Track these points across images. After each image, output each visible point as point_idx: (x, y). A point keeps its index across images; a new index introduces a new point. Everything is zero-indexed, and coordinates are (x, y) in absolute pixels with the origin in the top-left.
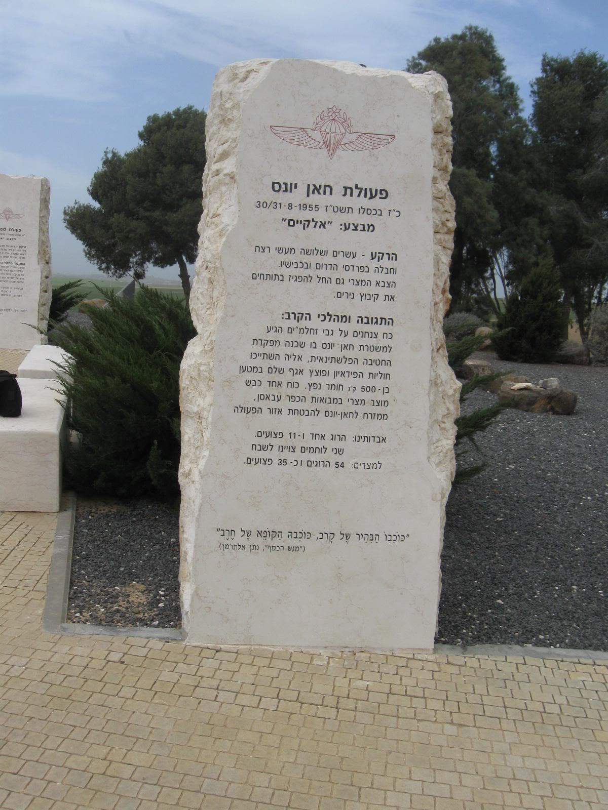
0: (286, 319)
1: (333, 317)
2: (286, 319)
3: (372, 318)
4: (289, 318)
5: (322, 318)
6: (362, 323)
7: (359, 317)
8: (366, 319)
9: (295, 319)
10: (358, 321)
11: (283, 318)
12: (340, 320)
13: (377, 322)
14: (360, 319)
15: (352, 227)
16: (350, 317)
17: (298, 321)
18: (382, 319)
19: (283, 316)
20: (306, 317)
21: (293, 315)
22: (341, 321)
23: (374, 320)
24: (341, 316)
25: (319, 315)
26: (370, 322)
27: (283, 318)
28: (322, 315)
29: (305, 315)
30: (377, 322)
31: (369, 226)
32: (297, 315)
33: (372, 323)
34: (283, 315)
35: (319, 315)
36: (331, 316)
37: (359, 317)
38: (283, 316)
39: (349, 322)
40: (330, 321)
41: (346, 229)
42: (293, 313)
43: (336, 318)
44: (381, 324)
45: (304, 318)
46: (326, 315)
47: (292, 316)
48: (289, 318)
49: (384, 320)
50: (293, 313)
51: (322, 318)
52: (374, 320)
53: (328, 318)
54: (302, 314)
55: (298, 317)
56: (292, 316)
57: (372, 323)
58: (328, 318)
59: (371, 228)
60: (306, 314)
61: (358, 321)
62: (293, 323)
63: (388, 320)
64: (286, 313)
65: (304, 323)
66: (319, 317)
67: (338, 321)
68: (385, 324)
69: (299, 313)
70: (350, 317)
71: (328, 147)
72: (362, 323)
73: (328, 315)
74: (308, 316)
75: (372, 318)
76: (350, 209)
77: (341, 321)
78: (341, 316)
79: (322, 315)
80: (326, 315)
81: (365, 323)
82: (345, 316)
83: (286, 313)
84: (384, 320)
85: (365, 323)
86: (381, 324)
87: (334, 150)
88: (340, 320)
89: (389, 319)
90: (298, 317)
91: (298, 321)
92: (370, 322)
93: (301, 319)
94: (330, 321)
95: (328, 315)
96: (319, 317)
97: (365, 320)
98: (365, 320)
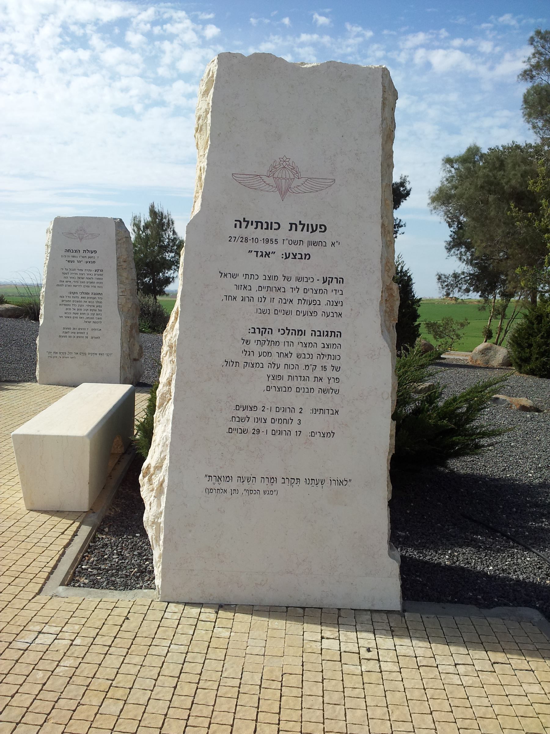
0: (252, 333)
1: (291, 331)
2: (252, 333)
3: (324, 331)
4: (255, 332)
5: (282, 332)
6: (315, 336)
7: (312, 331)
9: (259, 333)
10: (312, 334)
11: (249, 332)
12: (297, 334)
13: (327, 335)
14: (313, 332)
16: (305, 331)
17: (262, 335)
19: (250, 331)
22: (298, 335)
23: (326, 333)
25: (279, 329)
26: (322, 334)
27: (249, 332)
28: (282, 329)
29: (267, 330)
30: (327, 335)
32: (261, 330)
33: (323, 336)
34: (249, 329)
35: (279, 329)
36: (289, 330)
37: (312, 331)
38: (250, 331)
39: (305, 335)
42: (257, 328)
43: (294, 332)
45: (267, 332)
47: (257, 331)
48: (255, 332)
49: (333, 333)
50: (257, 328)
51: (282, 332)
52: (326, 333)
54: (266, 329)
55: (262, 331)
56: (257, 331)
57: (323, 336)
61: (312, 334)
62: (258, 336)
63: (336, 333)
64: (252, 328)
65: (266, 336)
66: (279, 331)
67: (295, 335)
68: (335, 336)
70: (305, 331)
71: (281, 193)
72: (315, 336)
73: (287, 329)
74: (270, 330)
75: (324, 331)
76: (301, 242)
77: (298, 335)
79: (282, 329)
80: (285, 330)
81: (318, 336)
82: (301, 330)
83: (252, 328)
84: (333, 333)
85: (318, 336)
87: (285, 193)
88: (297, 334)
89: (337, 332)
90: (262, 331)
91: (262, 335)
92: (322, 334)
93: (265, 333)
94: (288, 335)
95: (287, 329)
96: (279, 331)
97: (318, 333)
98: (318, 333)
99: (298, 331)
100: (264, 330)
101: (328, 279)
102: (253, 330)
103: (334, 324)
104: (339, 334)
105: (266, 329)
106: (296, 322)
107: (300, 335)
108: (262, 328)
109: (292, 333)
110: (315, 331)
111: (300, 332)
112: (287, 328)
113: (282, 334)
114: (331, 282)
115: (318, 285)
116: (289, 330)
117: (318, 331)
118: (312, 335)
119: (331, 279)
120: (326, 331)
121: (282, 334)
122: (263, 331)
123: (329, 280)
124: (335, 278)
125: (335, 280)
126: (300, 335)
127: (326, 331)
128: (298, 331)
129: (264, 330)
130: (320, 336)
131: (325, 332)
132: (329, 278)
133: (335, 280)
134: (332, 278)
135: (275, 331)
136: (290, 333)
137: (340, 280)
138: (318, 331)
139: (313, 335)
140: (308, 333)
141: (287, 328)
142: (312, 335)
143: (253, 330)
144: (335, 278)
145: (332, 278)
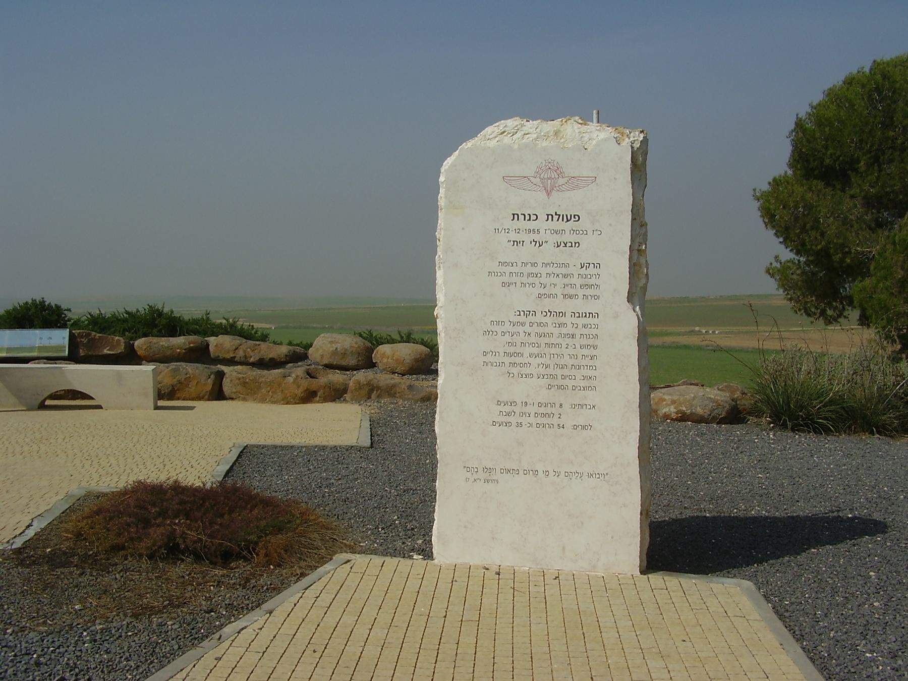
1: (553, 313)
14: (573, 314)
15: (563, 244)
18: (589, 313)
20: (532, 314)
23: (584, 315)
29: (531, 312)
30: (586, 316)
31: (575, 243)
32: (526, 312)
36: (551, 312)
41: (558, 246)
43: (555, 314)
45: (531, 314)
47: (522, 313)
48: (520, 315)
49: (591, 315)
52: (584, 315)
53: (549, 314)
54: (530, 312)
56: (522, 313)
58: (549, 314)
59: (577, 245)
62: (522, 318)
82: (562, 312)
84: (591, 315)
95: (549, 311)
97: (577, 315)
100: (528, 313)
101: (585, 265)
103: (592, 307)
104: (596, 315)
105: (530, 312)
106: (558, 305)
116: (551, 312)
119: (588, 265)
122: (527, 313)
130: (579, 317)
134: (589, 264)
136: (552, 315)
137: (597, 266)
140: (568, 315)
145: (589, 264)
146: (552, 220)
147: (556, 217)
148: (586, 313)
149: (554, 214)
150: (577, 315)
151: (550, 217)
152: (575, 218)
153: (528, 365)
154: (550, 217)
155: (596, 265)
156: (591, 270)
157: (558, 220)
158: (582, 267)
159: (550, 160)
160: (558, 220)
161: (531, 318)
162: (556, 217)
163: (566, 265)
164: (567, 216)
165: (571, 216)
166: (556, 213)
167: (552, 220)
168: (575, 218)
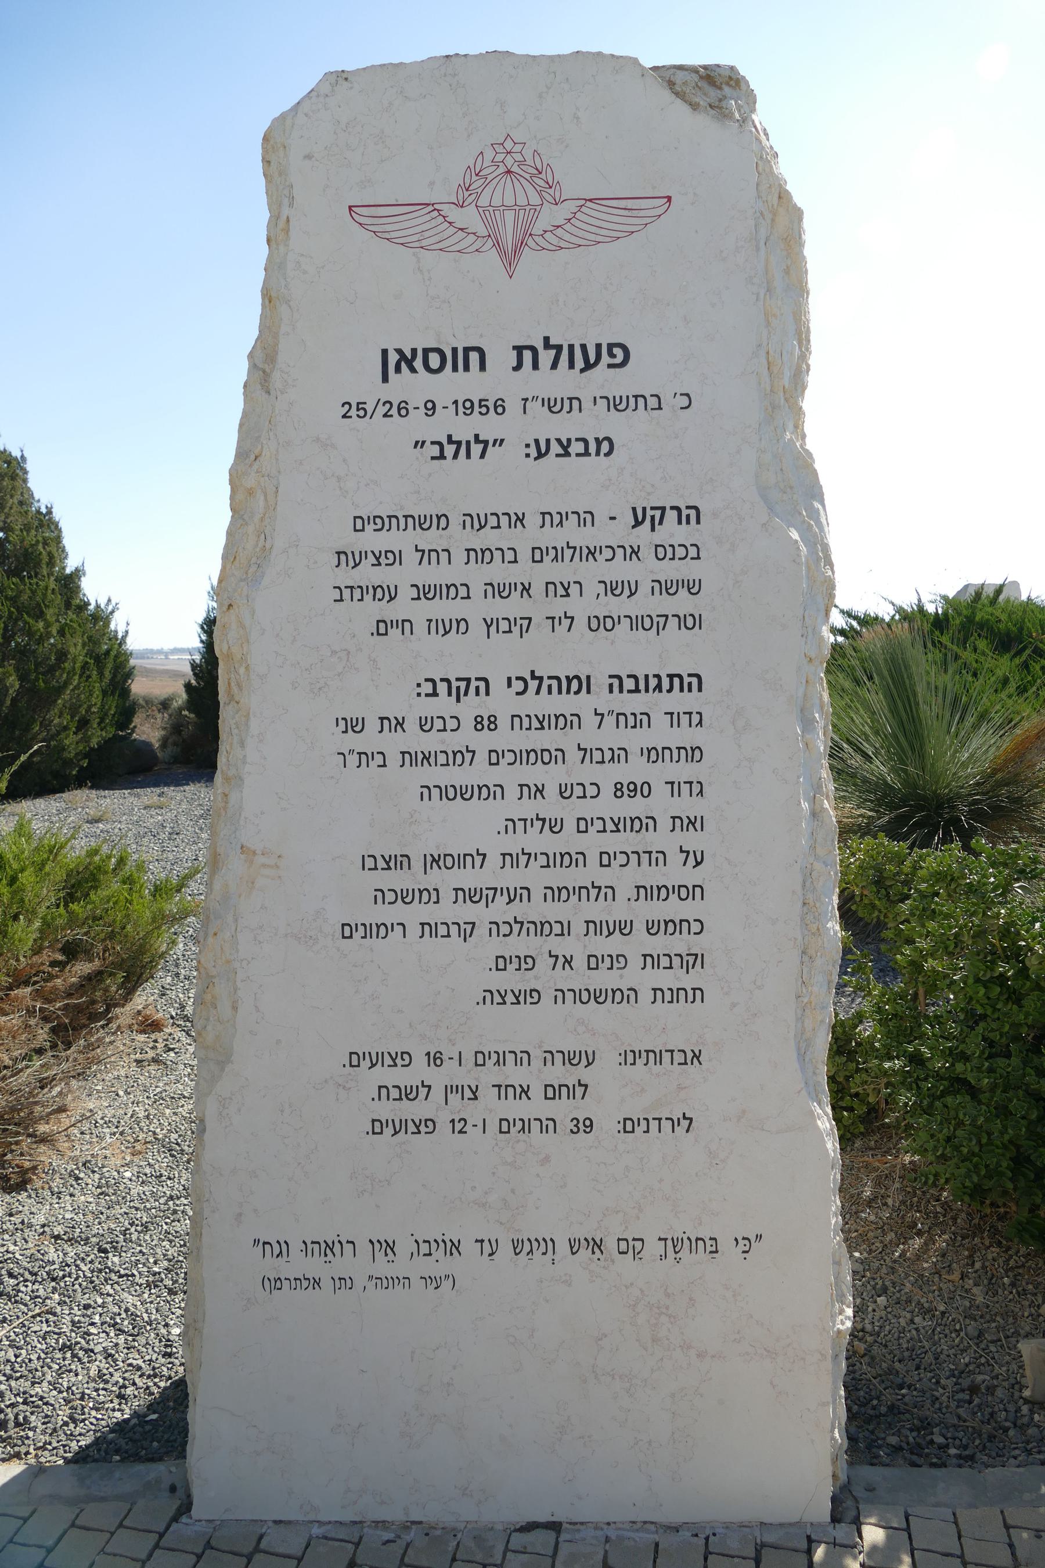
0: (427, 695)
1: (546, 682)
2: (427, 695)
3: (647, 676)
4: (435, 694)
5: (519, 686)
7: (610, 677)
8: (632, 680)
9: (450, 694)
10: (611, 686)
11: (419, 695)
13: (659, 687)
14: (616, 682)
17: (458, 700)
18: (671, 677)
19: (419, 690)
21: (445, 684)
22: (568, 692)
23: (653, 683)
24: (567, 677)
26: (642, 686)
27: (419, 695)
28: (518, 678)
29: (474, 684)
30: (659, 687)
32: (455, 684)
33: (647, 690)
34: (419, 685)
35: (509, 679)
36: (541, 679)
38: (419, 690)
39: (589, 692)
40: (538, 692)
42: (442, 680)
43: (554, 683)
44: (670, 691)
45: (472, 690)
46: (528, 677)
47: (442, 687)
48: (435, 694)
49: (676, 681)
50: (442, 680)
51: (519, 686)
52: (653, 683)
53: (533, 685)
55: (458, 688)
56: (442, 687)
57: (647, 690)
58: (533, 685)
60: (477, 679)
61: (611, 686)
62: (444, 704)
63: (686, 680)
64: (427, 680)
66: (509, 685)
67: (560, 692)
68: (682, 690)
69: (458, 679)
70: (588, 678)
72: (621, 691)
74: (482, 685)
75: (647, 676)
77: (568, 692)
78: (567, 677)
79: (518, 678)
80: (528, 677)
81: (629, 691)
83: (427, 680)
84: (676, 681)
85: (629, 691)
86: (670, 691)
89: (690, 675)
90: (458, 688)
91: (458, 700)
92: (642, 686)
93: (466, 694)
94: (538, 692)
95: (533, 676)
96: (509, 685)
97: (629, 684)
99: (569, 680)
100: (463, 685)
101: (649, 513)
102: (428, 688)
104: (694, 681)
107: (577, 693)
108: (458, 679)
109: (550, 686)
110: (619, 678)
111: (575, 683)
112: (533, 672)
113: (518, 694)
114: (661, 523)
115: (621, 533)
116: (541, 679)
117: (629, 676)
118: (611, 691)
119: (658, 514)
120: (655, 676)
121: (518, 694)
123: (653, 518)
124: (672, 508)
125: (671, 516)
126: (576, 693)
127: (655, 676)
128: (569, 680)
129: (463, 685)
130: (637, 690)
131: (651, 678)
132: (652, 508)
133: (671, 516)
134: (663, 509)
135: (498, 685)
138: (629, 676)
139: (616, 689)
141: (533, 672)
142: (611, 691)
143: (428, 688)
144: (672, 508)
146: (535, 366)
147: (546, 357)
148: (656, 676)
149: (539, 345)
150: (629, 684)
151: (527, 355)
152: (612, 355)
153: (478, 860)
154: (527, 355)
155: (685, 512)
156: (671, 531)
157: (554, 366)
158: (638, 523)
159: (509, 145)
160: (554, 366)
161: (471, 706)
162: (546, 357)
163: (586, 518)
164: (584, 347)
165: (599, 346)
166: (546, 339)
167: (535, 366)
168: (612, 355)
